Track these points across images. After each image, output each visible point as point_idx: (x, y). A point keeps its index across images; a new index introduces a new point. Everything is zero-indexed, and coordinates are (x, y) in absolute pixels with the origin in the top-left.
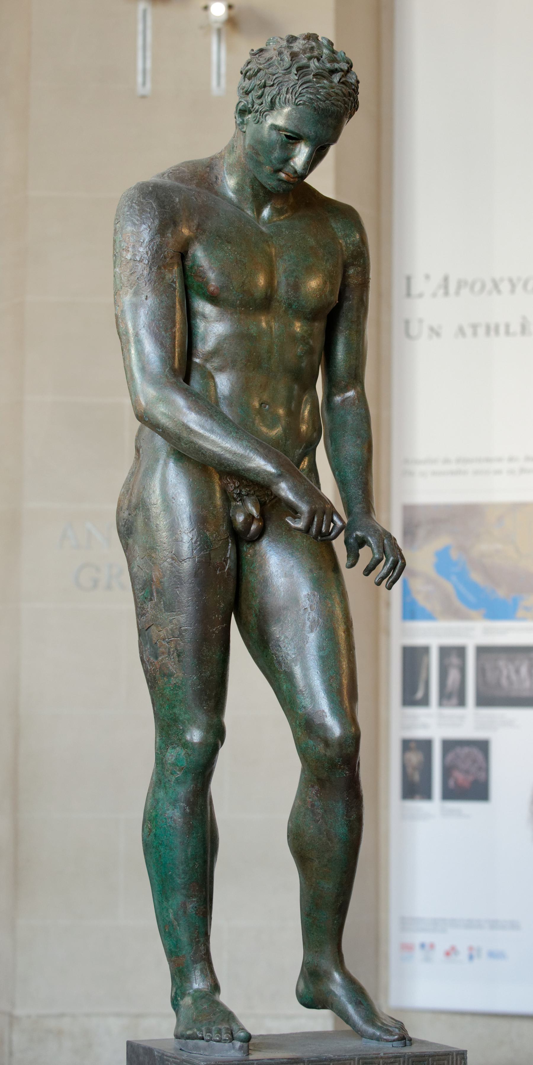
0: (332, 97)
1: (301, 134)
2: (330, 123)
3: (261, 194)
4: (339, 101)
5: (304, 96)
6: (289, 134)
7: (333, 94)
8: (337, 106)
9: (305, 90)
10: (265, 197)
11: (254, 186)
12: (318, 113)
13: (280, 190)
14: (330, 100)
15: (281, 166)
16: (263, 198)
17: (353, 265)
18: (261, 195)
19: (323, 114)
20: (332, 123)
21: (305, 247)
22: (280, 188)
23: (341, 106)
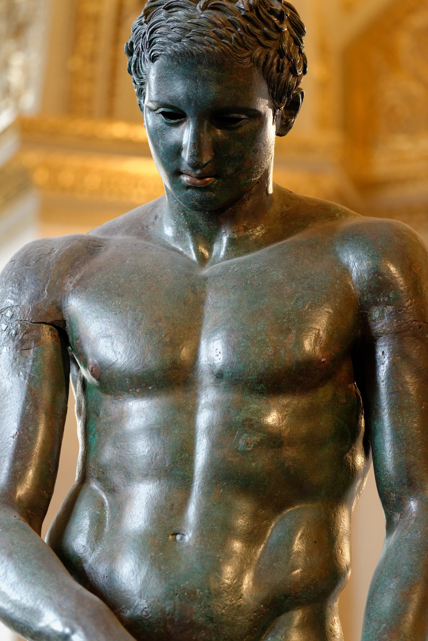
0: (190, 31)
1: (168, 102)
2: (205, 74)
3: (201, 222)
4: (205, 35)
5: (155, 43)
6: (161, 110)
7: (190, 25)
8: (202, 43)
9: (154, 35)
10: (209, 225)
11: (187, 212)
12: (179, 62)
13: (193, 204)
14: (188, 37)
15: (175, 163)
16: (206, 228)
17: (376, 304)
18: (201, 225)
19: (186, 62)
20: (207, 73)
21: (259, 284)
22: (192, 200)
23: (211, 43)
